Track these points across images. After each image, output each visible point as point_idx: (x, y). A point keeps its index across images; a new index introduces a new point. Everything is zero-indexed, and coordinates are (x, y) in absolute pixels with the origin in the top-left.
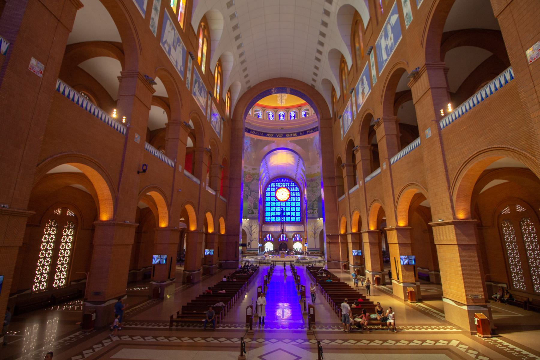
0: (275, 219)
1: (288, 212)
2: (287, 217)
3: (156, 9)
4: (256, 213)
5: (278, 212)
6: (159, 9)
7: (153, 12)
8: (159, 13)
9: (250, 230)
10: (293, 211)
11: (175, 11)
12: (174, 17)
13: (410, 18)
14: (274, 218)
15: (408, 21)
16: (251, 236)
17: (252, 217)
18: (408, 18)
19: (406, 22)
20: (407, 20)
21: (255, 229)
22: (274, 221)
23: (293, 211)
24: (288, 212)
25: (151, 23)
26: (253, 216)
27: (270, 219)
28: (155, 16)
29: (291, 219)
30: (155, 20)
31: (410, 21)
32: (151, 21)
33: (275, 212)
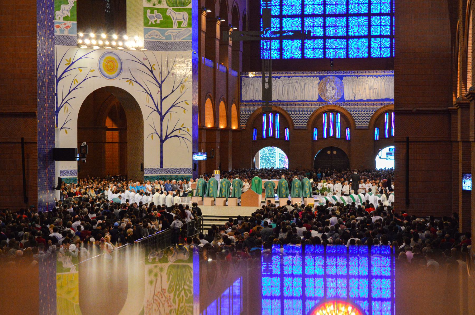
0: (302, 49)
1: (358, 15)
2: (288, 38)
4: (180, 23)
5: (313, 16)
9: (157, 98)
10: (380, 14)
14: (297, 43)
16: (162, 118)
17: (163, 40)
21: (177, 93)
22: (298, 55)
23: (380, 14)
24: (358, 15)
26: (169, 37)
27: (281, 49)
29: (369, 47)
33: (303, 16)
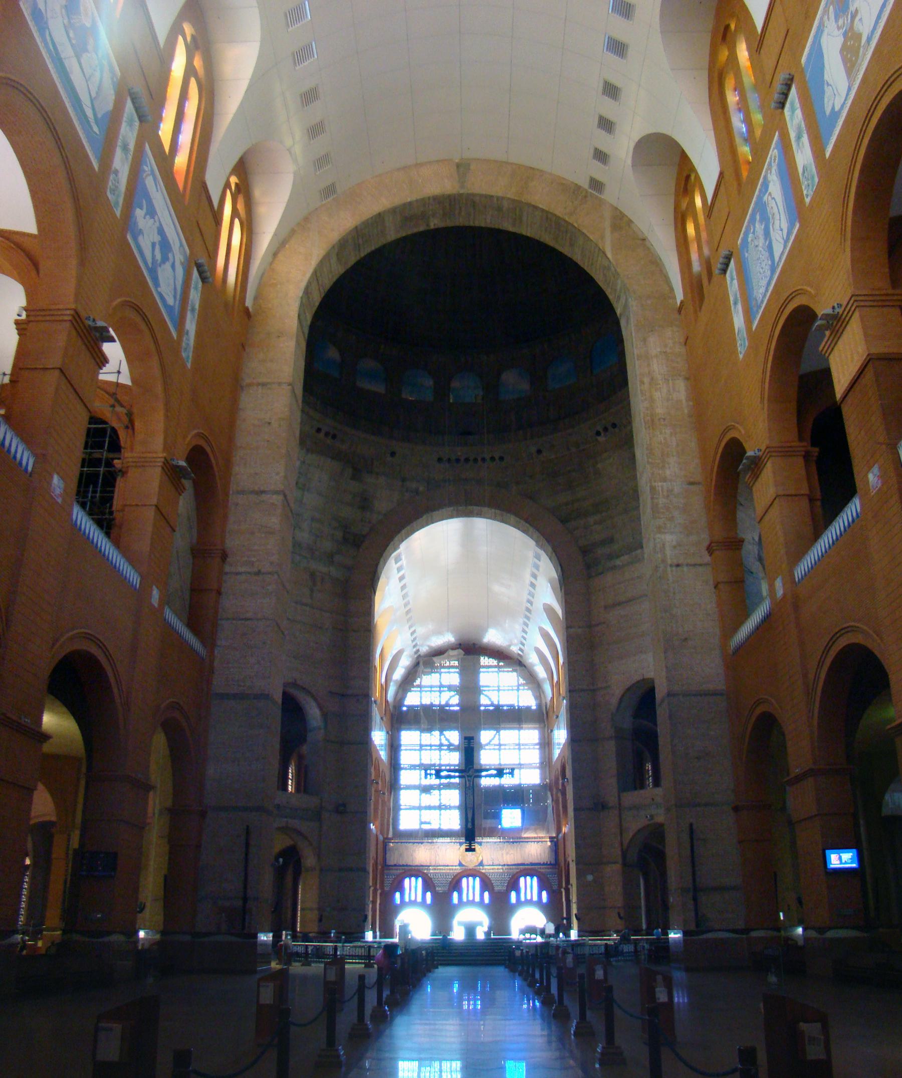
3: (125, 148)
6: (132, 147)
7: (119, 154)
8: (130, 157)
11: (167, 148)
12: (165, 161)
13: (813, 177)
15: (809, 185)
18: (808, 180)
19: (803, 187)
20: (806, 183)
25: (110, 183)
28: (121, 164)
30: (120, 175)
31: (813, 187)
32: (112, 177)
